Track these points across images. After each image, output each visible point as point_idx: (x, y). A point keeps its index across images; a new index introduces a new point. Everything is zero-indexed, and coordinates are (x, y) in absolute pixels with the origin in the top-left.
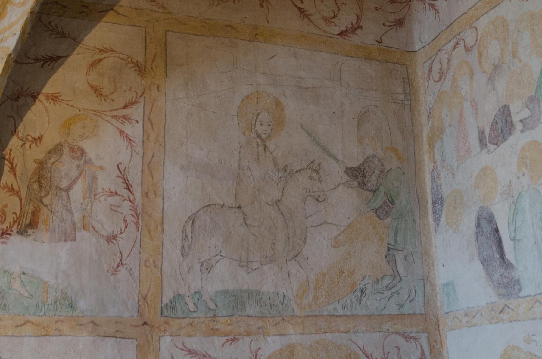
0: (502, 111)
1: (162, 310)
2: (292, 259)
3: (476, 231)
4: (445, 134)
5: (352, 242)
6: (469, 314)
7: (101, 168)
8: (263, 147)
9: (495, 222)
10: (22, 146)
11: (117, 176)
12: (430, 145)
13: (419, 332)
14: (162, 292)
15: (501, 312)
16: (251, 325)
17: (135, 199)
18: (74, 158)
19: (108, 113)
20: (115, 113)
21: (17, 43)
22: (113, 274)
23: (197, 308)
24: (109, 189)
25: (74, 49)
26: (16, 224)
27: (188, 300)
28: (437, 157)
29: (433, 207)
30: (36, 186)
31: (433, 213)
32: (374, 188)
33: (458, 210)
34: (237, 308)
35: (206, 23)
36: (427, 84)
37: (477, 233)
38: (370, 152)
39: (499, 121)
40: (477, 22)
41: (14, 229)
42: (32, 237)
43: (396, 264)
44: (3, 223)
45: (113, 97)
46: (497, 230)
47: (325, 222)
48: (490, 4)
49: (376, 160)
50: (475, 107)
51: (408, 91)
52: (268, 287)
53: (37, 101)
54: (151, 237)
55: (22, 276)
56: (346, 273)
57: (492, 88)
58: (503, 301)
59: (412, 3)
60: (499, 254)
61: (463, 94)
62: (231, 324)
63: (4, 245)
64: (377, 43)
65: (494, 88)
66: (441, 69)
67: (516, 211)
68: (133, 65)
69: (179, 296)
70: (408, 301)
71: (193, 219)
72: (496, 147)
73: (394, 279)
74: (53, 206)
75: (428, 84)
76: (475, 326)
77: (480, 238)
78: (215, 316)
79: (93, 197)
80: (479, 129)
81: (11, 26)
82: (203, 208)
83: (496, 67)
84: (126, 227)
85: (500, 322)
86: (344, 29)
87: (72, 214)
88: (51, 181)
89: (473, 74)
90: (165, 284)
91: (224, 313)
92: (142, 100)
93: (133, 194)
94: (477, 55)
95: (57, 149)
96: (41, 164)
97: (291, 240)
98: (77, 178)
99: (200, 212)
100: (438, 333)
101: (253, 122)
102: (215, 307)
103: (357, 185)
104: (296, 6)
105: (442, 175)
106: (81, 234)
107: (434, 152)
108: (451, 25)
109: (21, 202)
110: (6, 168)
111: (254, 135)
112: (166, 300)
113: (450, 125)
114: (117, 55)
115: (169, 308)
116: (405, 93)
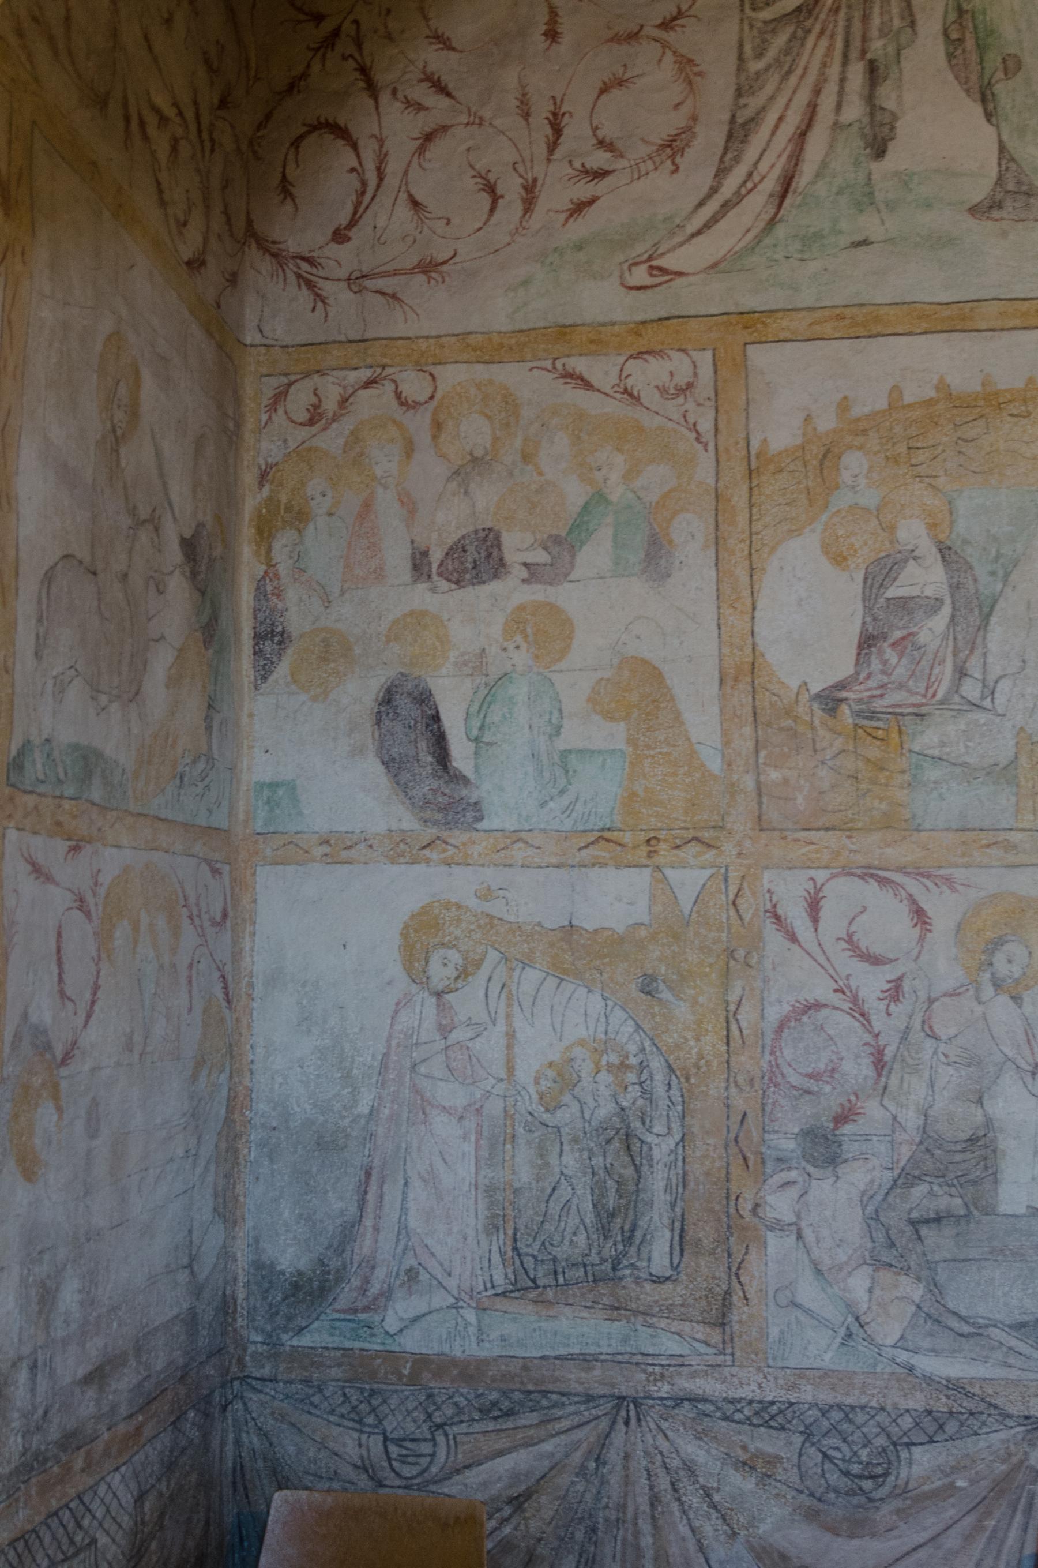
0: (482, 534)
3: (376, 710)
6: (332, 842)
9: (435, 704)
12: (260, 531)
15: (424, 848)
29: (257, 644)
31: (255, 653)
33: (332, 665)
36: (264, 418)
37: (379, 712)
39: (471, 549)
40: (439, 367)
46: (436, 718)
48: (478, 353)
50: (410, 507)
57: (462, 490)
58: (433, 832)
60: (434, 757)
61: (378, 471)
65: (466, 493)
67: (489, 699)
72: (454, 586)
75: (270, 417)
76: (350, 863)
77: (386, 722)
80: (415, 545)
85: (419, 863)
89: (413, 450)
94: (428, 420)
105: (292, 594)
108: (360, 341)
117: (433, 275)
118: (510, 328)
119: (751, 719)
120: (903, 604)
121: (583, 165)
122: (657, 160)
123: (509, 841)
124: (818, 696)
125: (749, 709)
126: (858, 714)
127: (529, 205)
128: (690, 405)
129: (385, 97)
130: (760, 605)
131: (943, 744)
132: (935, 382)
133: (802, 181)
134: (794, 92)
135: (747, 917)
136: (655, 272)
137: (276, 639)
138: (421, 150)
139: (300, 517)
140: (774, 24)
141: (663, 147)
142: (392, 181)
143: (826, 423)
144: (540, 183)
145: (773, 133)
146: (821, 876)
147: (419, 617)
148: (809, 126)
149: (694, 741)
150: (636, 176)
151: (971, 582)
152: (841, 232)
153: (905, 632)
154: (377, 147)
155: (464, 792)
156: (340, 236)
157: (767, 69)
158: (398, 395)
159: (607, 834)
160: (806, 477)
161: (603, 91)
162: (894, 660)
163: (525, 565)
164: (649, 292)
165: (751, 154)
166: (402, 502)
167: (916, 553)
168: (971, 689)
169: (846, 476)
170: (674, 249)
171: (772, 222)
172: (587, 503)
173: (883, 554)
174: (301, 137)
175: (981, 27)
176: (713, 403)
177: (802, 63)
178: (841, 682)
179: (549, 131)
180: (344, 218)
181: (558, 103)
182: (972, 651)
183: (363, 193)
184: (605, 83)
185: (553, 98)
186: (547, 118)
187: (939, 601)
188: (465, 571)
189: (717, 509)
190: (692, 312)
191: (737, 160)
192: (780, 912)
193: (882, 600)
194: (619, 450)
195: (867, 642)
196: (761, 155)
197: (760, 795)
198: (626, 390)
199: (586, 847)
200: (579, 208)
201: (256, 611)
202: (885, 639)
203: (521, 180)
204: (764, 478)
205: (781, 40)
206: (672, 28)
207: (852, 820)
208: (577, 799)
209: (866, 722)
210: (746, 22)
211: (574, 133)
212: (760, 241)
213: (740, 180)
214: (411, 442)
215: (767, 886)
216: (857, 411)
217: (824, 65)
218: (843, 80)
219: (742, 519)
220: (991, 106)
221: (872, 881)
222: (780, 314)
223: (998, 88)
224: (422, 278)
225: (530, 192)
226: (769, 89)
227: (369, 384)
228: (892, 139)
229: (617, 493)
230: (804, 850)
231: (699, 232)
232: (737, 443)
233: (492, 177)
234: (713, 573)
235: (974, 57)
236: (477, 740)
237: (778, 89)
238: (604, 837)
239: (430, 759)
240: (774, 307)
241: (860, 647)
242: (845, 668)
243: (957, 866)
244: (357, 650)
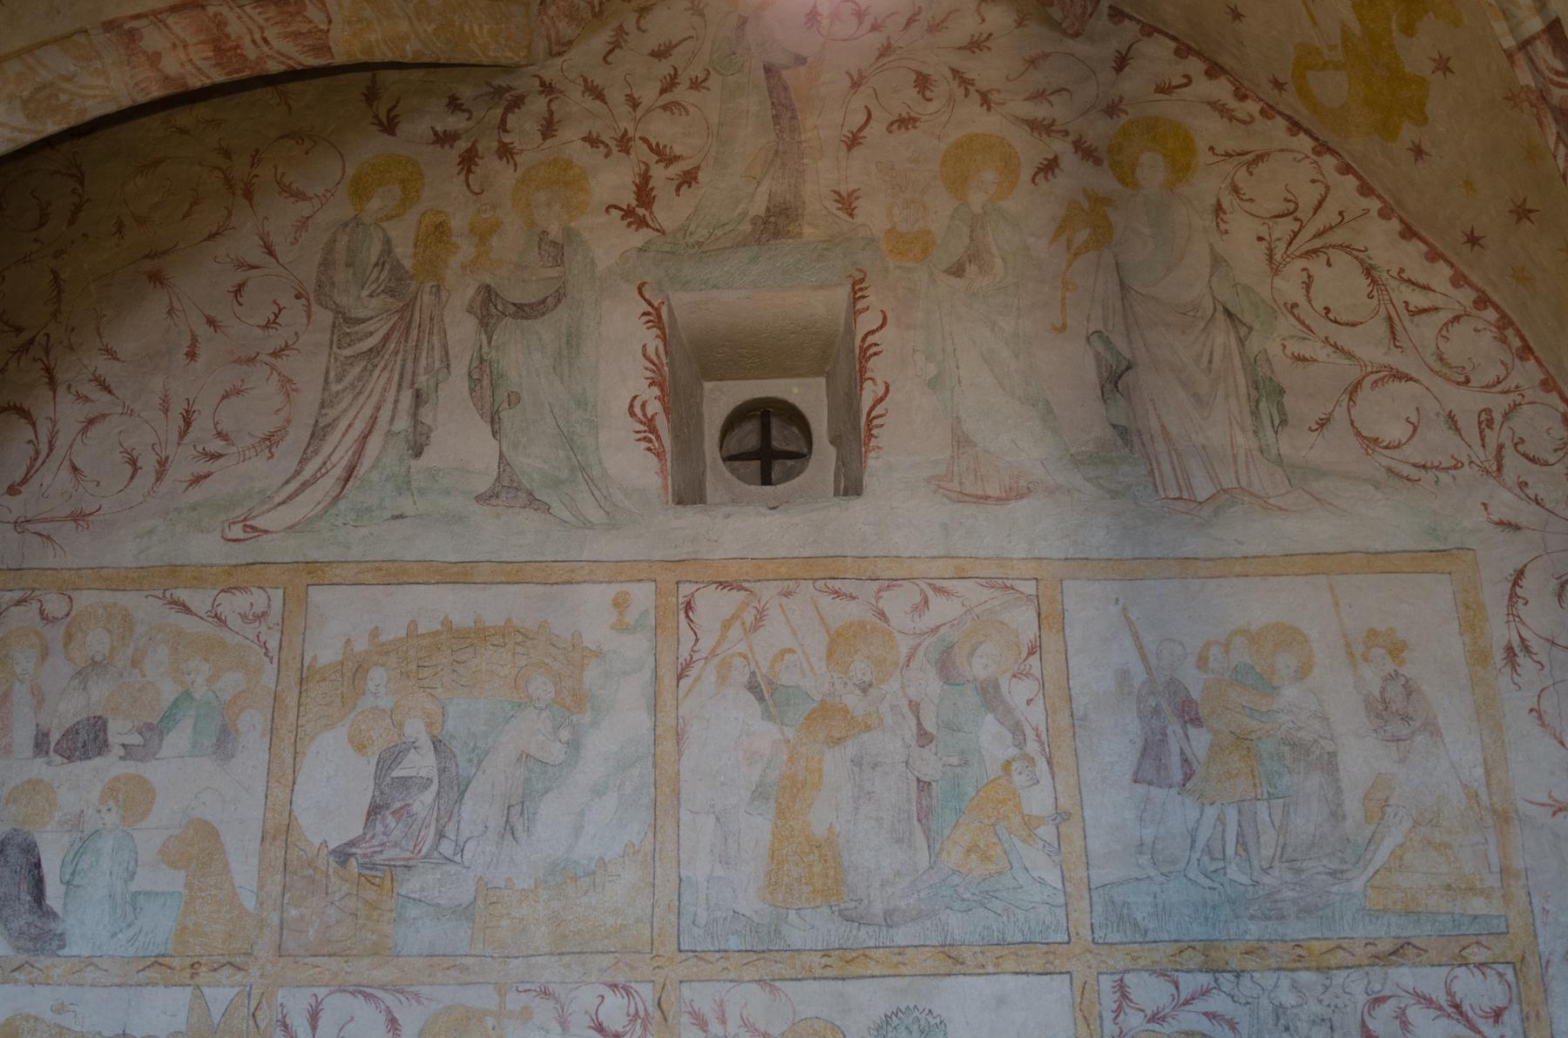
0: (92, 721)
9: (38, 854)
15: (14, 971)
46: (38, 865)
50: (39, 698)
57: (82, 687)
58: (23, 957)
61: (18, 671)
65: (84, 689)
67: (81, 851)
72: (65, 761)
83: (96, 666)
89: (47, 654)
108: (18, 569)
117: (81, 522)
118: (135, 565)
119: (281, 869)
120: (404, 782)
122: (259, 449)
123: (83, 965)
124: (334, 852)
125: (280, 862)
126: (362, 866)
128: (263, 629)
129: (61, 390)
130: (299, 780)
131: (422, 889)
132: (441, 619)
133: (361, 470)
134: (362, 407)
135: (262, 1025)
136: (248, 530)
138: (84, 431)
140: (352, 359)
141: (264, 439)
142: (59, 451)
143: (361, 646)
145: (343, 435)
146: (322, 992)
147: (34, 785)
148: (370, 432)
149: (236, 885)
150: (242, 459)
151: (454, 767)
152: (385, 508)
153: (403, 803)
155: (53, 925)
157: (344, 390)
158: (42, 612)
159: (161, 960)
160: (343, 685)
161: (224, 397)
162: (393, 825)
163: (123, 745)
164: (242, 544)
165: (327, 449)
166: (34, 694)
167: (417, 744)
168: (447, 848)
169: (371, 685)
170: (263, 513)
171: (337, 498)
172: (177, 699)
173: (393, 744)
175: (495, 372)
176: (280, 628)
177: (370, 388)
178: (352, 841)
179: (182, 423)
180: (18, 476)
181: (191, 402)
182: (450, 819)
183: (36, 459)
187: (430, 780)
188: (76, 749)
189: (274, 707)
190: (272, 561)
191: (316, 452)
192: (288, 1021)
193: (388, 780)
194: (206, 660)
195: (375, 810)
196: (335, 449)
197: (282, 929)
198: (216, 615)
199: (143, 970)
200: (198, 479)
202: (388, 808)
204: (311, 685)
205: (357, 370)
206: (280, 357)
207: (349, 948)
208: (140, 931)
209: (368, 872)
210: (333, 356)
211: (202, 425)
212: (327, 511)
213: (317, 467)
214: (47, 648)
215: (280, 1001)
216: (383, 638)
217: (385, 390)
218: (396, 402)
219: (292, 716)
220: (497, 426)
221: (360, 996)
222: (335, 565)
223: (503, 414)
224: (73, 524)
225: (163, 464)
226: (344, 404)
227: (19, 603)
228: (427, 445)
229: (200, 692)
230: (311, 972)
231: (283, 503)
232: (295, 658)
233: (135, 453)
234: (267, 756)
235: (489, 392)
236: (68, 883)
237: (351, 405)
238: (158, 962)
239: (29, 898)
240: (331, 559)
241: (369, 814)
242: (356, 830)
243: (423, 984)
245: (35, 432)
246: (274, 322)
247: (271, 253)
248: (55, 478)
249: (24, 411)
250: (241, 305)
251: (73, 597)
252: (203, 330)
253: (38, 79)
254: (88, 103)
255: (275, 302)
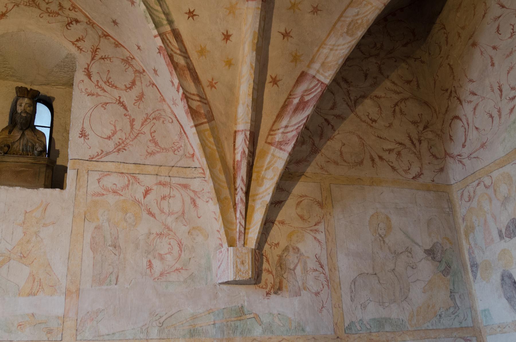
0: (512, 221)
1: (345, 331)
2: (404, 300)
4: (475, 230)
5: (432, 290)
6: (501, 326)
7: (308, 257)
8: (383, 241)
10: (270, 248)
11: (316, 261)
12: (466, 235)
13: (472, 337)
14: (344, 321)
16: (388, 336)
17: (326, 273)
18: (295, 253)
19: (308, 229)
20: (311, 228)
21: (271, 198)
22: (320, 312)
23: (361, 328)
24: (313, 268)
25: (288, 197)
26: (273, 289)
27: (357, 324)
28: (471, 241)
29: (472, 269)
30: (279, 268)
31: (472, 272)
32: (439, 260)
33: (488, 271)
34: (381, 327)
35: (347, 178)
36: (460, 203)
37: (502, 283)
38: (435, 240)
39: (511, 226)
40: (492, 173)
41: (272, 291)
42: (280, 295)
43: (455, 300)
44: (266, 289)
45: (309, 220)
47: (418, 280)
49: (439, 245)
50: (494, 217)
51: (450, 207)
52: (394, 316)
53: (274, 224)
54: (336, 292)
55: (279, 315)
56: (431, 306)
59: (446, 158)
61: (486, 210)
62: (379, 336)
63: (269, 300)
64: (432, 182)
65: (506, 209)
66: (469, 195)
68: (317, 203)
69: (352, 323)
70: (464, 320)
71: (354, 281)
72: (510, 239)
73: (455, 309)
74: (288, 279)
75: (461, 203)
78: (371, 332)
79: (306, 273)
81: (266, 190)
82: (358, 275)
83: (506, 199)
84: (323, 287)
86: (415, 176)
87: (298, 282)
88: (286, 265)
90: (345, 317)
91: (375, 330)
92: (323, 221)
93: (324, 270)
94: (493, 190)
95: (286, 249)
96: (280, 257)
97: (402, 290)
98: (298, 263)
99: (357, 277)
100: (481, 337)
101: (377, 229)
102: (370, 328)
103: (431, 259)
104: (390, 165)
105: (476, 252)
106: (303, 292)
107: (469, 239)
108: (474, 173)
109: (274, 277)
110: (264, 260)
111: (378, 235)
112: (346, 325)
113: (478, 226)
114: (308, 198)
115: (348, 329)
116: (449, 208)
121: (509, 98)
127: (500, 116)
129: (463, 103)
137: (475, 266)
138: (474, 113)
139: (473, 228)
144: (501, 108)
154: (465, 118)
156: (464, 146)
161: (508, 73)
174: (451, 123)
179: (499, 92)
183: (466, 131)
184: (508, 71)
185: (498, 82)
186: (498, 89)
200: (512, 110)
201: (470, 259)
203: (497, 109)
211: (506, 88)
224: (482, 149)
227: (478, 184)
233: (490, 112)
244: (493, 265)
245: (462, 122)
246: (513, 32)
247: (503, 7)
248: (473, 135)
249: (457, 117)
250: (500, 34)
251: (491, 175)
252: (492, 52)
253: (347, 23)
254: (369, 17)
255: (511, 25)
